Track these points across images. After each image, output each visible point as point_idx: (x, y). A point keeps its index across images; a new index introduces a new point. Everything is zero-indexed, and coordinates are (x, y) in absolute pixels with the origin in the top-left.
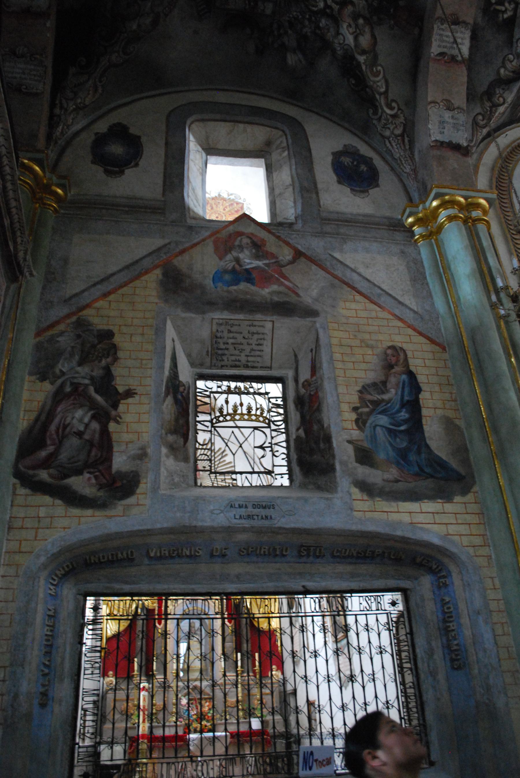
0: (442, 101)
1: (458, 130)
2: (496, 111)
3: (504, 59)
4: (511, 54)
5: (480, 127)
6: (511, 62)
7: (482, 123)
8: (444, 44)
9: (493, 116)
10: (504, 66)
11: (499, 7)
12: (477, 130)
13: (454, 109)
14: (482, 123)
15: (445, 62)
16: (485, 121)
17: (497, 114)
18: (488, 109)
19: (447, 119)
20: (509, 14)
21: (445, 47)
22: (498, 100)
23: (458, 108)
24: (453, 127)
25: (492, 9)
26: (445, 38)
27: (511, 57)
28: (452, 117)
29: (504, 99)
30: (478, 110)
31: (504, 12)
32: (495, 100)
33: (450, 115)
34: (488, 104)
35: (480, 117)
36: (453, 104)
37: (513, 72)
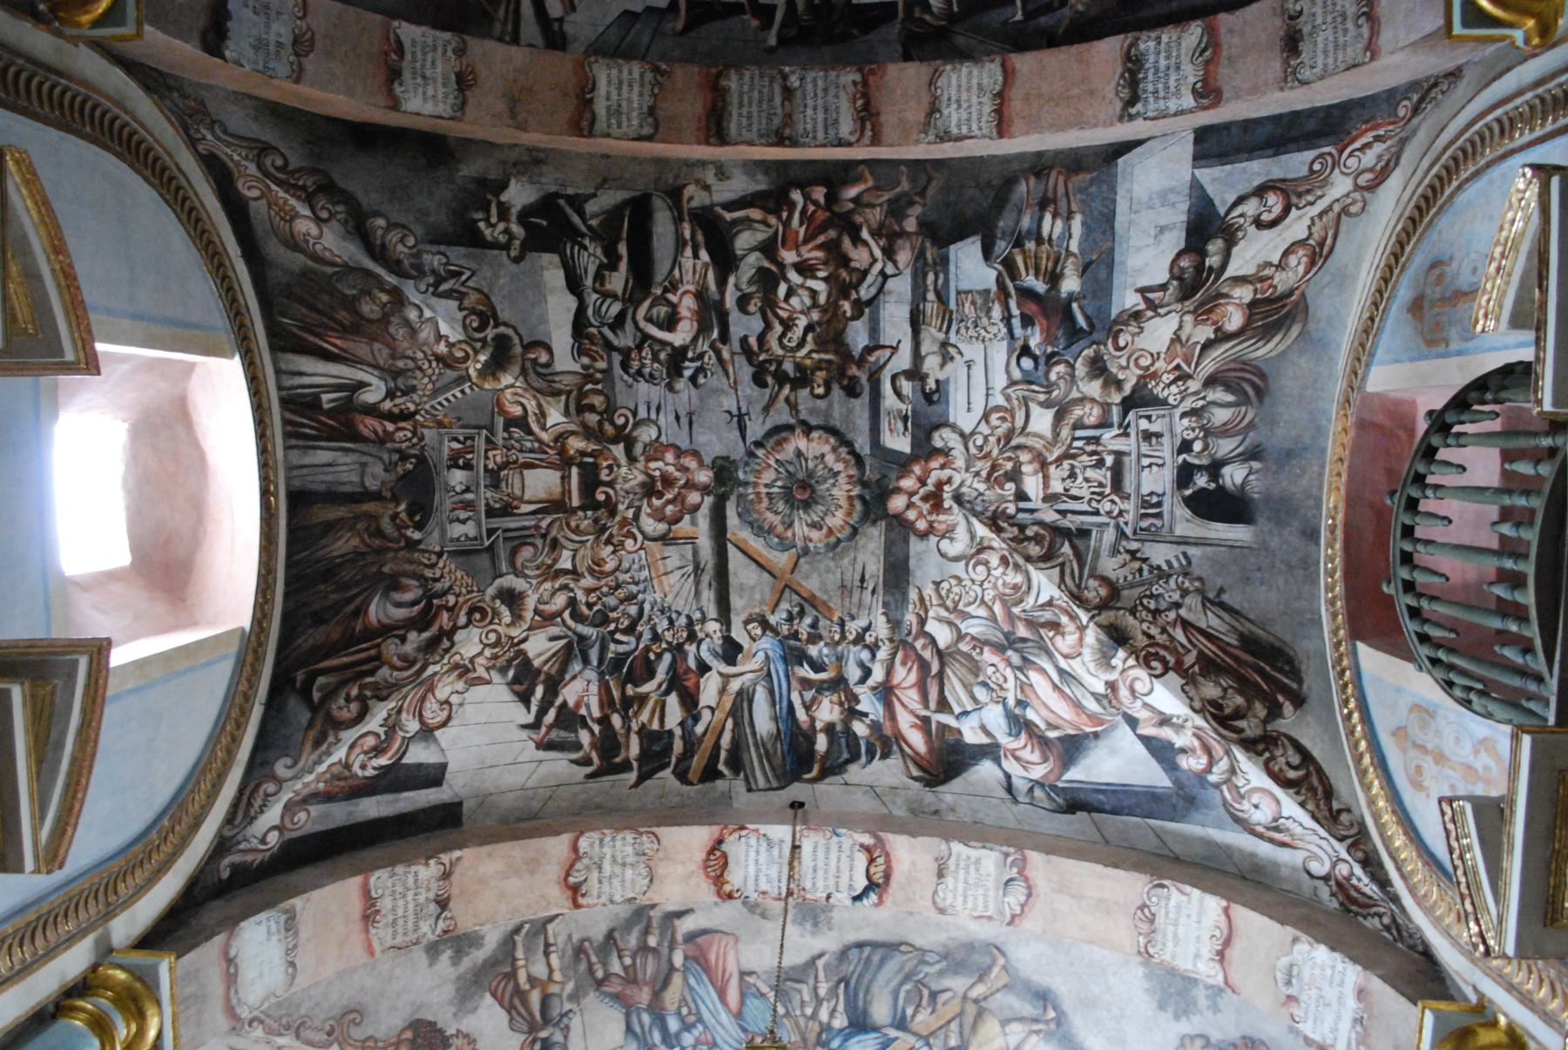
0: (309, 28)
1: (254, 47)
2: (299, 198)
3: (404, 227)
4: (417, 243)
5: (259, 156)
6: (402, 240)
7: (268, 162)
8: (419, 56)
9: (287, 191)
10: (392, 226)
11: (494, 211)
12: (252, 149)
13: (296, 54)
14: (268, 162)
15: (386, 54)
16: (272, 170)
17: (292, 201)
18: (301, 183)
19: (275, 27)
20: (487, 232)
21: (413, 53)
22: (323, 208)
23: (301, 69)
24: (259, 40)
25: (489, 196)
26: (429, 57)
27: (411, 241)
28: (279, 44)
29: (326, 221)
30: (294, 163)
31: (487, 220)
32: (322, 201)
33: (283, 40)
34: (309, 182)
35: (279, 162)
36: (307, 55)
37: (383, 245)
